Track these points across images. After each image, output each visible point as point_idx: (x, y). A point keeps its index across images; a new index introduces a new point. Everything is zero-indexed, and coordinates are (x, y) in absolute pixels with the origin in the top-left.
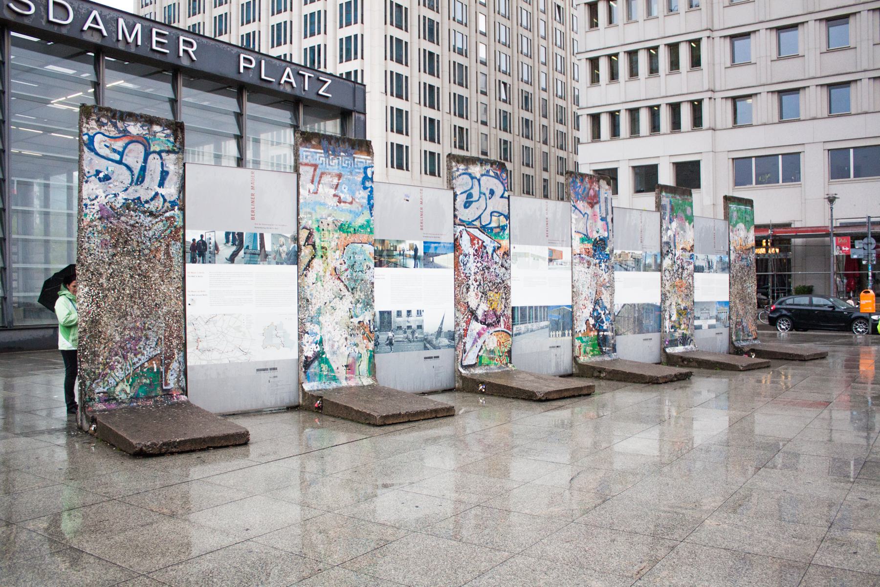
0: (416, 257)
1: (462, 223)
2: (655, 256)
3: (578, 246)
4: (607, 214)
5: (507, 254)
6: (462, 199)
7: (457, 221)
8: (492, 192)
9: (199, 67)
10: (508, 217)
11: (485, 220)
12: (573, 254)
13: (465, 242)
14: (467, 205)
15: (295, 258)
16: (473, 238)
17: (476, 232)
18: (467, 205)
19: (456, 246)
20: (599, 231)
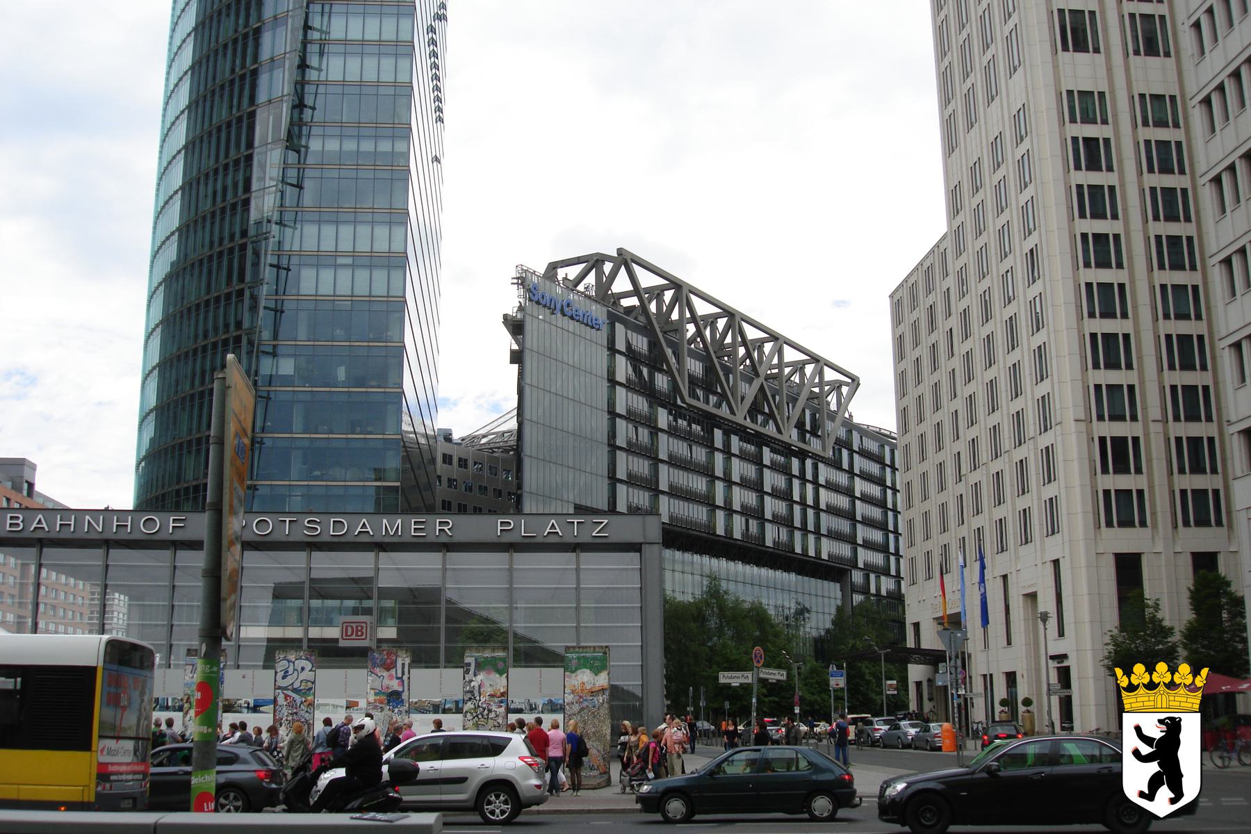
0: (248, 708)
1: (280, 688)
2: (457, 702)
3: (372, 698)
4: (403, 673)
5: (311, 704)
6: (280, 675)
7: (277, 688)
8: (303, 669)
9: (455, 540)
10: (313, 683)
11: (296, 685)
12: (369, 703)
13: (281, 700)
14: (284, 678)
15: (180, 709)
16: (286, 696)
17: (290, 693)
18: (284, 678)
19: (275, 701)
20: (395, 685)
